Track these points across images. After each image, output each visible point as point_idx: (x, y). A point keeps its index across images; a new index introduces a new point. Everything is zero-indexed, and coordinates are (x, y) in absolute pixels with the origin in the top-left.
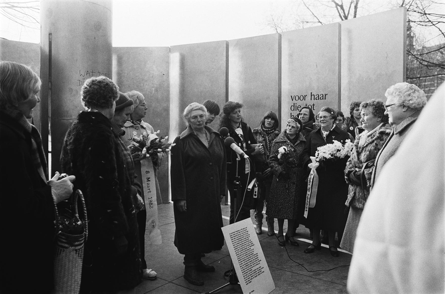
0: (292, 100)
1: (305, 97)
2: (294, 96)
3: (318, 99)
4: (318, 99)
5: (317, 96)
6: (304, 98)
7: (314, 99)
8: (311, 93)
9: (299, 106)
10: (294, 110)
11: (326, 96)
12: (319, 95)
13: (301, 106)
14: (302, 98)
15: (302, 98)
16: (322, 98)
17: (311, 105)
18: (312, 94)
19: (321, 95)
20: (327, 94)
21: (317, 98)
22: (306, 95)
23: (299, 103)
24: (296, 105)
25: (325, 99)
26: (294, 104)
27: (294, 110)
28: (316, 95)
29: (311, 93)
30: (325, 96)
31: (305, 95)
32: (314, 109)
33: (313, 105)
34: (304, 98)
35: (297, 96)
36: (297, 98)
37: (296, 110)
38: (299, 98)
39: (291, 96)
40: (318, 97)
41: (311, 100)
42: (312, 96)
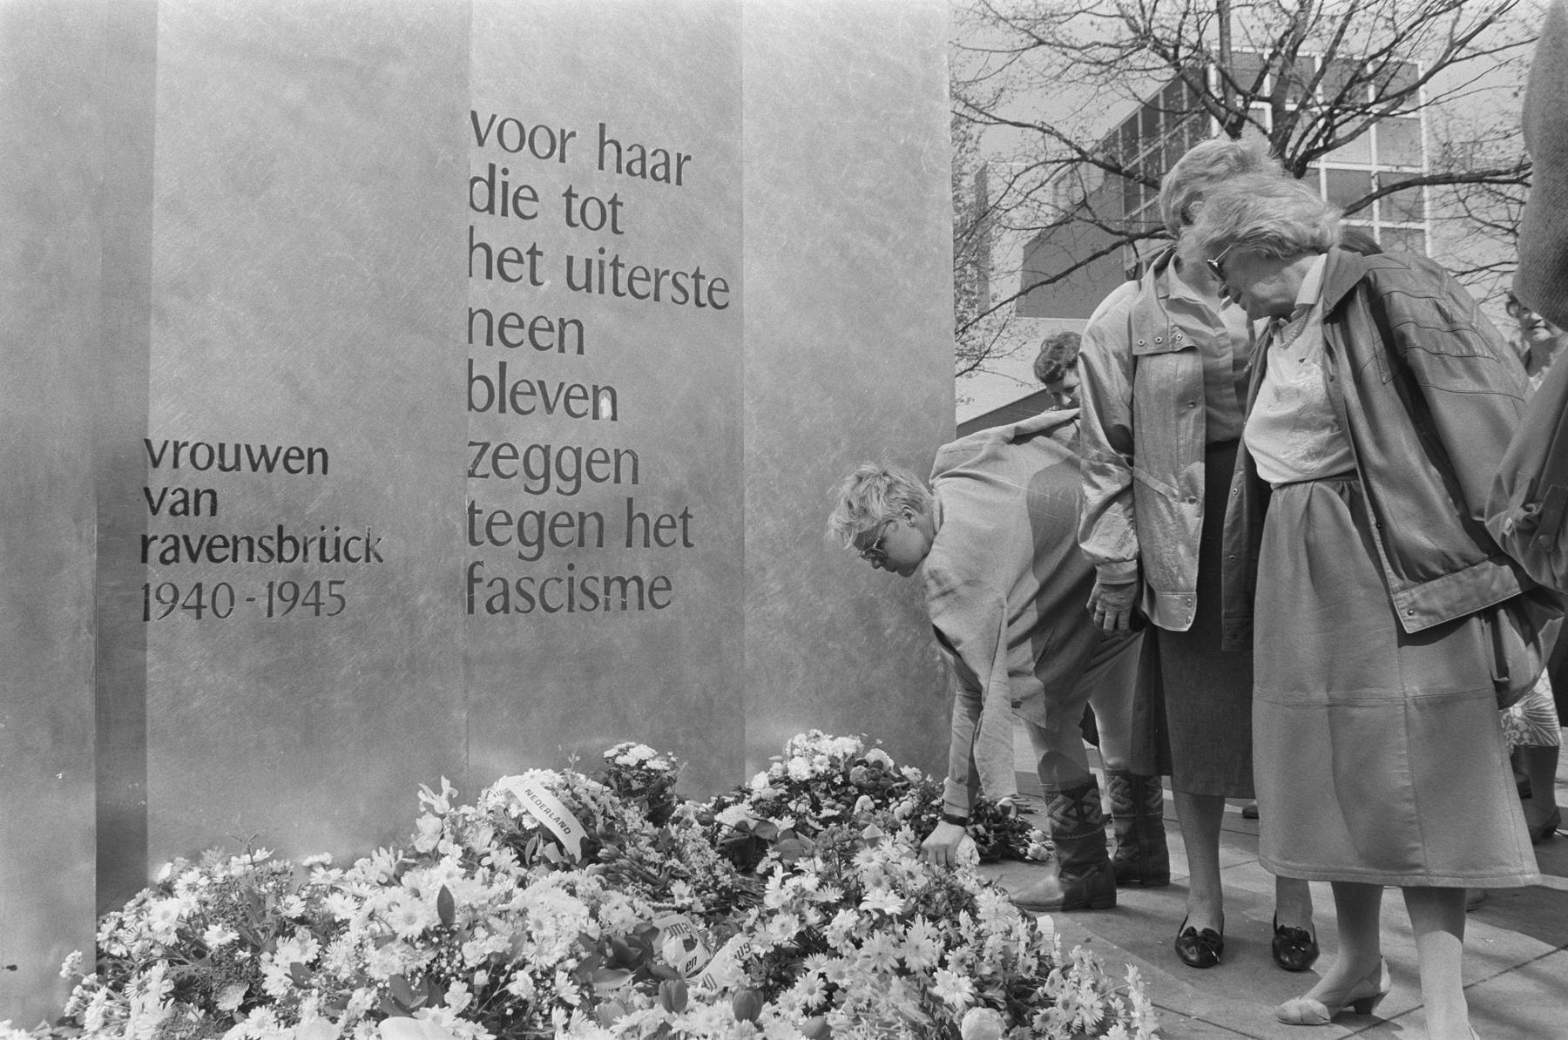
0: (481, 142)
1: (564, 141)
2: (494, 117)
3: (643, 174)
4: (643, 174)
5: (636, 153)
6: (557, 151)
7: (619, 171)
8: (602, 126)
9: (525, 193)
10: (492, 212)
12: (649, 152)
13: (539, 197)
14: (543, 147)
15: (543, 147)
16: (660, 172)
17: (600, 203)
18: (606, 139)
20: (688, 158)
21: (636, 168)
22: (573, 134)
23: (523, 170)
25: (679, 182)
26: (492, 167)
27: (490, 208)
29: (602, 126)
31: (563, 132)
34: (557, 151)
37: (504, 213)
38: (527, 139)
39: (474, 115)
41: (601, 167)
42: (606, 147)
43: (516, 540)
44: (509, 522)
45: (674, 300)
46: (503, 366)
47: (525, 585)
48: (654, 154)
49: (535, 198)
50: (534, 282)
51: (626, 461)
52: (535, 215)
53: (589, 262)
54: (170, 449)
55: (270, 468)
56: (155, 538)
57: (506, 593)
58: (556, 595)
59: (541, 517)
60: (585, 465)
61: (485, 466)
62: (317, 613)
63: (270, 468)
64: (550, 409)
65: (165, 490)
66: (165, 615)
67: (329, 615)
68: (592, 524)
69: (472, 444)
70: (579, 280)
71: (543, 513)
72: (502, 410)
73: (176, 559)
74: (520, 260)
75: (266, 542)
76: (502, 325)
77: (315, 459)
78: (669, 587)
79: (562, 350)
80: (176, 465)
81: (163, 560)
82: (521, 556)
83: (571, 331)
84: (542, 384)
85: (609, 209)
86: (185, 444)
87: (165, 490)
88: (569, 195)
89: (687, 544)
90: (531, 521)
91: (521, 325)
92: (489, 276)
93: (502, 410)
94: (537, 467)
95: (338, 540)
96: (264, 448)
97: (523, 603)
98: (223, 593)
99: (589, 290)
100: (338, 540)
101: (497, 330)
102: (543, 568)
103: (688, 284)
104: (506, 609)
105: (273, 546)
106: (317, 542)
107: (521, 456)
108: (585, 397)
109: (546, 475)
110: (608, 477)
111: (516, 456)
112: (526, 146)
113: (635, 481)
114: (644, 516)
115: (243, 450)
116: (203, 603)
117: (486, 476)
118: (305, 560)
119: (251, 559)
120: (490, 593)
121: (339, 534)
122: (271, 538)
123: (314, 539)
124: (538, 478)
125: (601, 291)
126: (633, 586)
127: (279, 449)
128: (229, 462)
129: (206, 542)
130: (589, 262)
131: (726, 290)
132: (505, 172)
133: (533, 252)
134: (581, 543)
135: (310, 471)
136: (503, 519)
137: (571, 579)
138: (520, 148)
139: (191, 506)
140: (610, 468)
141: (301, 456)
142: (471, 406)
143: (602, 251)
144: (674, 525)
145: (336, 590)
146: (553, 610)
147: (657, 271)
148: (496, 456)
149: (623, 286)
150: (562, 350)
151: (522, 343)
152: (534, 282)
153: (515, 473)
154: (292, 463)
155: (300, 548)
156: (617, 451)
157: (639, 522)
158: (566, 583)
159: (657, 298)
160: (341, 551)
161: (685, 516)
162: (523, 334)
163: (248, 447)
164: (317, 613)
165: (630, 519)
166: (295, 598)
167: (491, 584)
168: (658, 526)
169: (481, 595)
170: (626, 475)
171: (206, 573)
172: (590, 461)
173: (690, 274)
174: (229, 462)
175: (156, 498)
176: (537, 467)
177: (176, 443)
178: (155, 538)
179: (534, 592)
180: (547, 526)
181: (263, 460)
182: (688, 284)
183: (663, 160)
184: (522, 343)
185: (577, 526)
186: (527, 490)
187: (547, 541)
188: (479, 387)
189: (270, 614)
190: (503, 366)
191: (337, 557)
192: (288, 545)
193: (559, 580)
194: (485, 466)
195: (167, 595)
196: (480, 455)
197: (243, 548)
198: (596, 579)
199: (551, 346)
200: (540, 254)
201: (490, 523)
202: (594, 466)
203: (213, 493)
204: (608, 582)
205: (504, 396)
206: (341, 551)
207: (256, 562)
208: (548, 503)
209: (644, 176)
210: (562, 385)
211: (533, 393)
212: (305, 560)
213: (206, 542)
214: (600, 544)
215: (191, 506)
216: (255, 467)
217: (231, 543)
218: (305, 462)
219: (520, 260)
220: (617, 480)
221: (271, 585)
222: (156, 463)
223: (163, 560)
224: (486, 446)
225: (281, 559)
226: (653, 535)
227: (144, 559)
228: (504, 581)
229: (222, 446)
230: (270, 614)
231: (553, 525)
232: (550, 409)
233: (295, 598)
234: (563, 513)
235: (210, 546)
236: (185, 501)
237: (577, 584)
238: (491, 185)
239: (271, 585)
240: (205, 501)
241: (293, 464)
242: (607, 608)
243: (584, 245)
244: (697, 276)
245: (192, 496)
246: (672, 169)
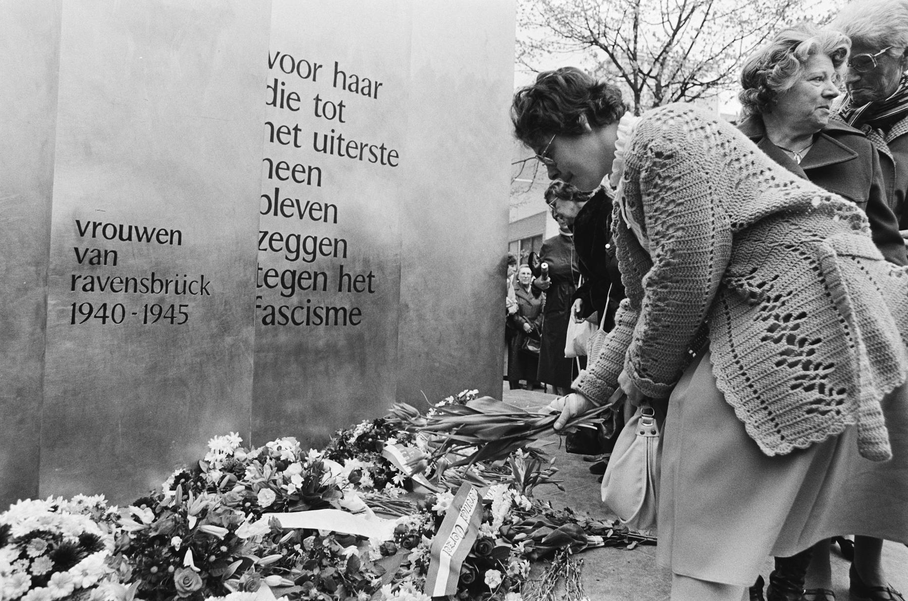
0: (271, 66)
1: (315, 70)
2: (278, 53)
4: (357, 91)
5: (354, 79)
7: (344, 88)
8: (336, 63)
9: (293, 96)
11: (380, 88)
12: (360, 80)
14: (304, 70)
15: (304, 70)
16: (366, 91)
19: (363, 81)
20: (381, 84)
21: (353, 87)
22: (321, 66)
23: (293, 83)
24: (283, 87)
25: (375, 97)
26: (276, 81)
27: (274, 103)
28: (351, 77)
29: (336, 63)
32: (343, 119)
33: (341, 105)
37: (282, 106)
38: (296, 67)
40: (357, 83)
41: (335, 85)
43: (280, 286)
44: (277, 275)
46: (277, 190)
47: (284, 310)
48: (363, 81)
49: (299, 100)
50: (296, 145)
52: (298, 109)
53: (326, 137)
54: (91, 226)
55: (148, 240)
56: (80, 277)
57: (273, 314)
58: (300, 316)
59: (294, 273)
62: (172, 322)
63: (148, 240)
64: (301, 216)
65: (87, 250)
66: (84, 321)
67: (179, 324)
68: (321, 279)
70: (320, 146)
71: (295, 272)
72: (276, 214)
73: (92, 289)
74: (289, 133)
75: (145, 282)
76: (278, 168)
77: (175, 237)
78: (360, 314)
79: (309, 183)
80: (94, 236)
81: (84, 289)
82: (282, 294)
83: (315, 173)
84: (297, 201)
85: (338, 108)
86: (100, 224)
87: (87, 250)
88: (317, 99)
89: (370, 291)
91: (288, 169)
92: (272, 140)
93: (276, 214)
94: (293, 247)
95: (185, 282)
96: (145, 228)
97: (283, 321)
98: (119, 310)
99: (325, 152)
100: (185, 282)
101: (274, 170)
102: (295, 300)
103: (378, 152)
104: (273, 322)
105: (149, 285)
106: (173, 284)
107: (285, 239)
108: (321, 210)
109: (298, 251)
110: (330, 253)
111: (282, 240)
112: (296, 69)
113: (345, 256)
114: (348, 275)
115: (134, 231)
116: (107, 315)
117: (265, 250)
118: (166, 293)
119: (135, 291)
120: (265, 313)
121: (185, 279)
122: (148, 280)
123: (172, 281)
124: (292, 252)
125: (332, 153)
126: (341, 312)
127: (154, 229)
128: (125, 236)
129: (110, 281)
130: (326, 137)
131: (397, 156)
132: (283, 84)
133: (296, 129)
134: (315, 288)
135: (171, 243)
136: (273, 273)
137: (308, 308)
138: (292, 71)
139: (102, 259)
140: (332, 249)
141: (167, 234)
143: (333, 131)
144: (364, 281)
145: (183, 309)
146: (299, 324)
147: (362, 144)
148: (271, 239)
149: (343, 151)
150: (309, 183)
151: (287, 178)
152: (296, 145)
153: (281, 249)
154: (161, 237)
155: (165, 285)
156: (336, 240)
157: (346, 278)
158: (305, 310)
159: (361, 159)
161: (370, 276)
162: (289, 173)
163: (136, 228)
164: (172, 322)
165: (341, 276)
166: (160, 314)
167: (265, 309)
168: (356, 281)
170: (340, 253)
171: (111, 299)
172: (321, 244)
173: (379, 146)
174: (125, 236)
175: (81, 254)
176: (293, 247)
177: (94, 223)
178: (80, 277)
180: (297, 278)
181: (145, 236)
182: (378, 152)
183: (368, 85)
184: (287, 178)
185: (312, 281)
186: (287, 258)
187: (297, 288)
189: (145, 322)
190: (277, 190)
191: (184, 292)
192: (157, 284)
193: (302, 308)
195: (86, 310)
197: (132, 283)
198: (322, 308)
199: (303, 181)
200: (300, 130)
201: (266, 276)
202: (323, 247)
203: (115, 252)
204: (328, 310)
206: (187, 288)
207: (138, 292)
209: (357, 92)
210: (308, 202)
211: (293, 206)
212: (166, 293)
213: (110, 281)
214: (325, 289)
215: (102, 259)
216: (140, 239)
217: (124, 281)
218: (168, 237)
219: (289, 133)
220: (335, 255)
221: (146, 306)
222: (82, 234)
223: (84, 289)
224: (266, 233)
225: (153, 291)
226: (353, 286)
227: (73, 289)
228: (273, 308)
229: (121, 227)
230: (145, 322)
231: (300, 278)
232: (301, 216)
233: (160, 314)
234: (305, 272)
235: (112, 283)
236: (99, 256)
237: (312, 310)
238: (275, 90)
239: (146, 306)
240: (111, 255)
241: (162, 238)
242: (327, 324)
243: (324, 127)
244: (383, 148)
245: (103, 253)
246: (372, 90)
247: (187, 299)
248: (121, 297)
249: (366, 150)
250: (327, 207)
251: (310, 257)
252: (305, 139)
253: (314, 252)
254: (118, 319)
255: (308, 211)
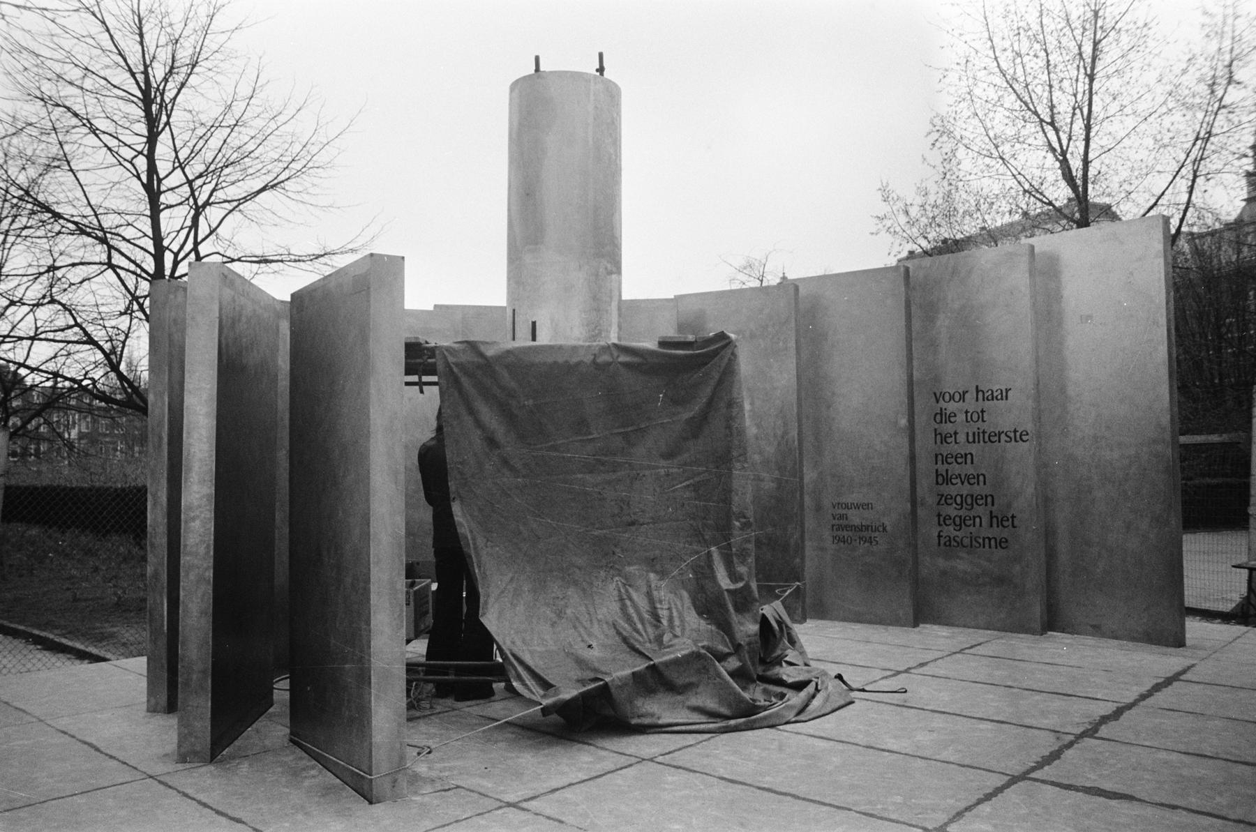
0: (938, 401)
4: (993, 399)
5: (990, 392)
16: (999, 397)
23: (951, 407)
25: (1007, 399)
26: (941, 409)
27: (941, 422)
30: (1007, 393)
33: (983, 411)
35: (947, 394)
36: (947, 398)
37: (946, 422)
38: (952, 398)
39: (935, 394)
40: (992, 394)
45: (1006, 441)
46: (947, 471)
49: (955, 416)
50: (956, 443)
51: (989, 499)
53: (974, 434)
57: (950, 541)
58: (966, 541)
59: (960, 517)
60: (975, 499)
61: (943, 502)
64: (963, 483)
68: (978, 520)
69: (938, 495)
72: (947, 484)
79: (966, 463)
83: (969, 456)
84: (960, 475)
85: (980, 414)
88: (967, 412)
90: (957, 519)
93: (947, 484)
97: (955, 544)
101: (945, 460)
103: (1012, 435)
104: (950, 545)
113: (993, 505)
114: (997, 517)
126: (993, 542)
131: (1027, 434)
140: (983, 501)
142: (937, 483)
144: (1008, 520)
149: (987, 439)
152: (956, 443)
160: (877, 530)
162: (953, 460)
169: (942, 542)
179: (958, 540)
182: (1012, 435)
188: (940, 480)
190: (947, 471)
194: (943, 502)
196: (941, 499)
205: (947, 480)
208: (962, 513)
214: (981, 525)
219: (951, 436)
224: (943, 495)
226: (1001, 523)
228: (950, 537)
231: (964, 520)
243: (973, 428)
244: (1015, 431)
247: (877, 534)
248: (850, 533)
249: (1003, 437)
250: (978, 476)
251: (969, 507)
252: (961, 438)
253: (972, 504)
254: (849, 541)
255: (968, 479)
